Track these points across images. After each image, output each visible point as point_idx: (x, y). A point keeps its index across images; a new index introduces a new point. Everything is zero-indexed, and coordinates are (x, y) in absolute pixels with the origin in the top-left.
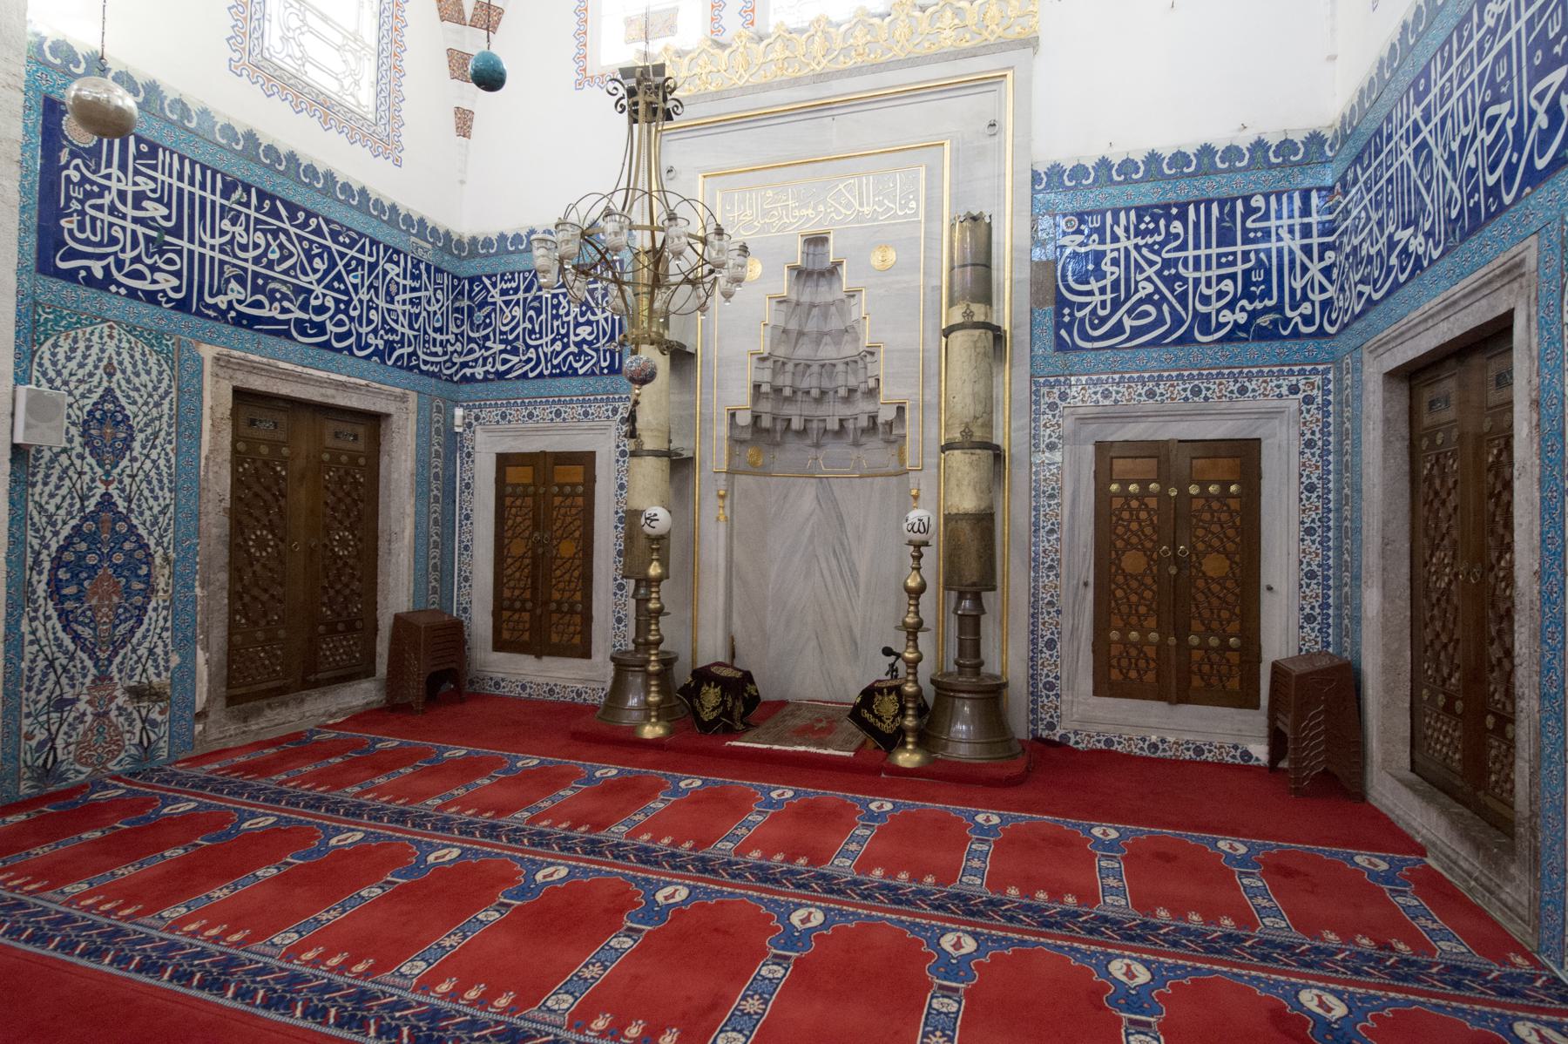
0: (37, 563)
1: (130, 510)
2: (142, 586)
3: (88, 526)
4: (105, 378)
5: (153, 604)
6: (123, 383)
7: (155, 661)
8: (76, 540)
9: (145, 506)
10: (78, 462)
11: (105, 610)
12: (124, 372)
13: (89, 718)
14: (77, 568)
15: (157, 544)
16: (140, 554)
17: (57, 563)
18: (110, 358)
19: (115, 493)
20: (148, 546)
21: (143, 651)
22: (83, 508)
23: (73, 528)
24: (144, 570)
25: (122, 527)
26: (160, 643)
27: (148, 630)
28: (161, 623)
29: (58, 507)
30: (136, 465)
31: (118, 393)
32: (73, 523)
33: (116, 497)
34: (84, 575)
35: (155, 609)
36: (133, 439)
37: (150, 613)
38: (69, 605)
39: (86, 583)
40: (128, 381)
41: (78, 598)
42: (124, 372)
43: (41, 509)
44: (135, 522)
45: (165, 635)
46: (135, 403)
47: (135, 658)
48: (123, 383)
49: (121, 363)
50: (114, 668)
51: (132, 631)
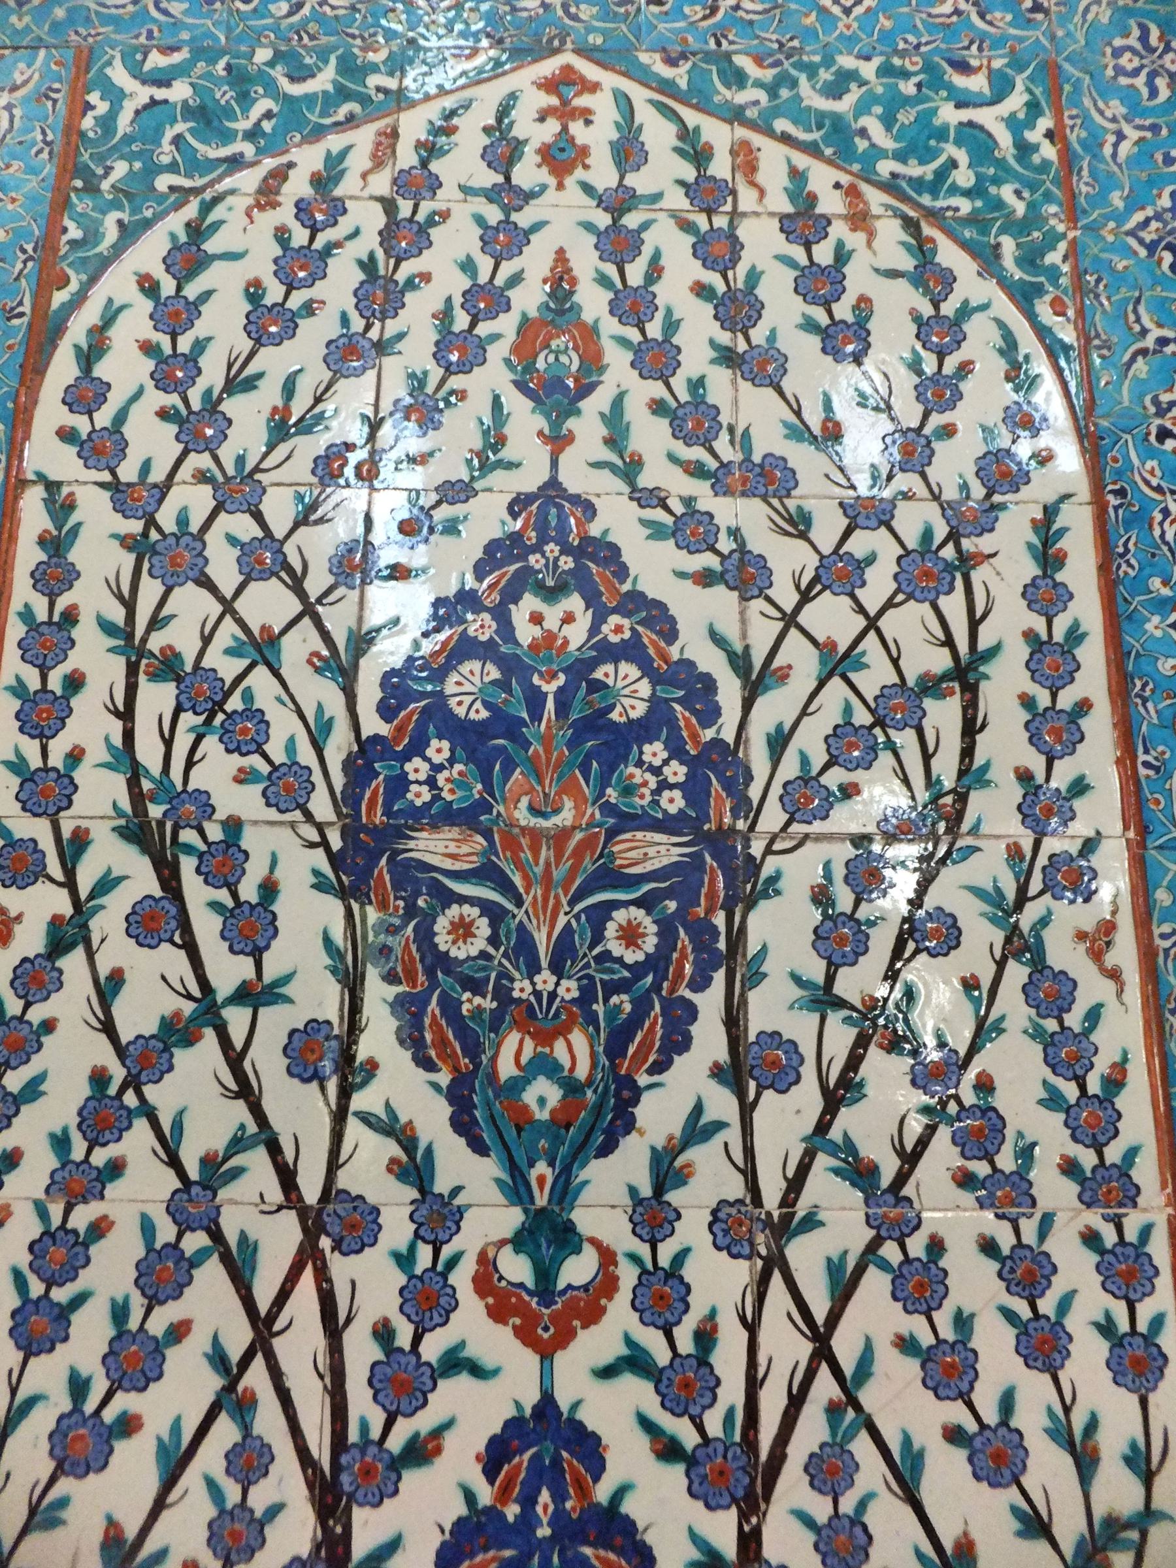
4: (525, 422)
6: (651, 437)
10: (299, 1111)
12: (657, 359)
18: (561, 281)
30: (785, 1119)
31: (618, 519)
33: (628, 1461)
36: (749, 886)
40: (693, 419)
42: (657, 359)
46: (745, 575)
48: (651, 437)
49: (633, 305)
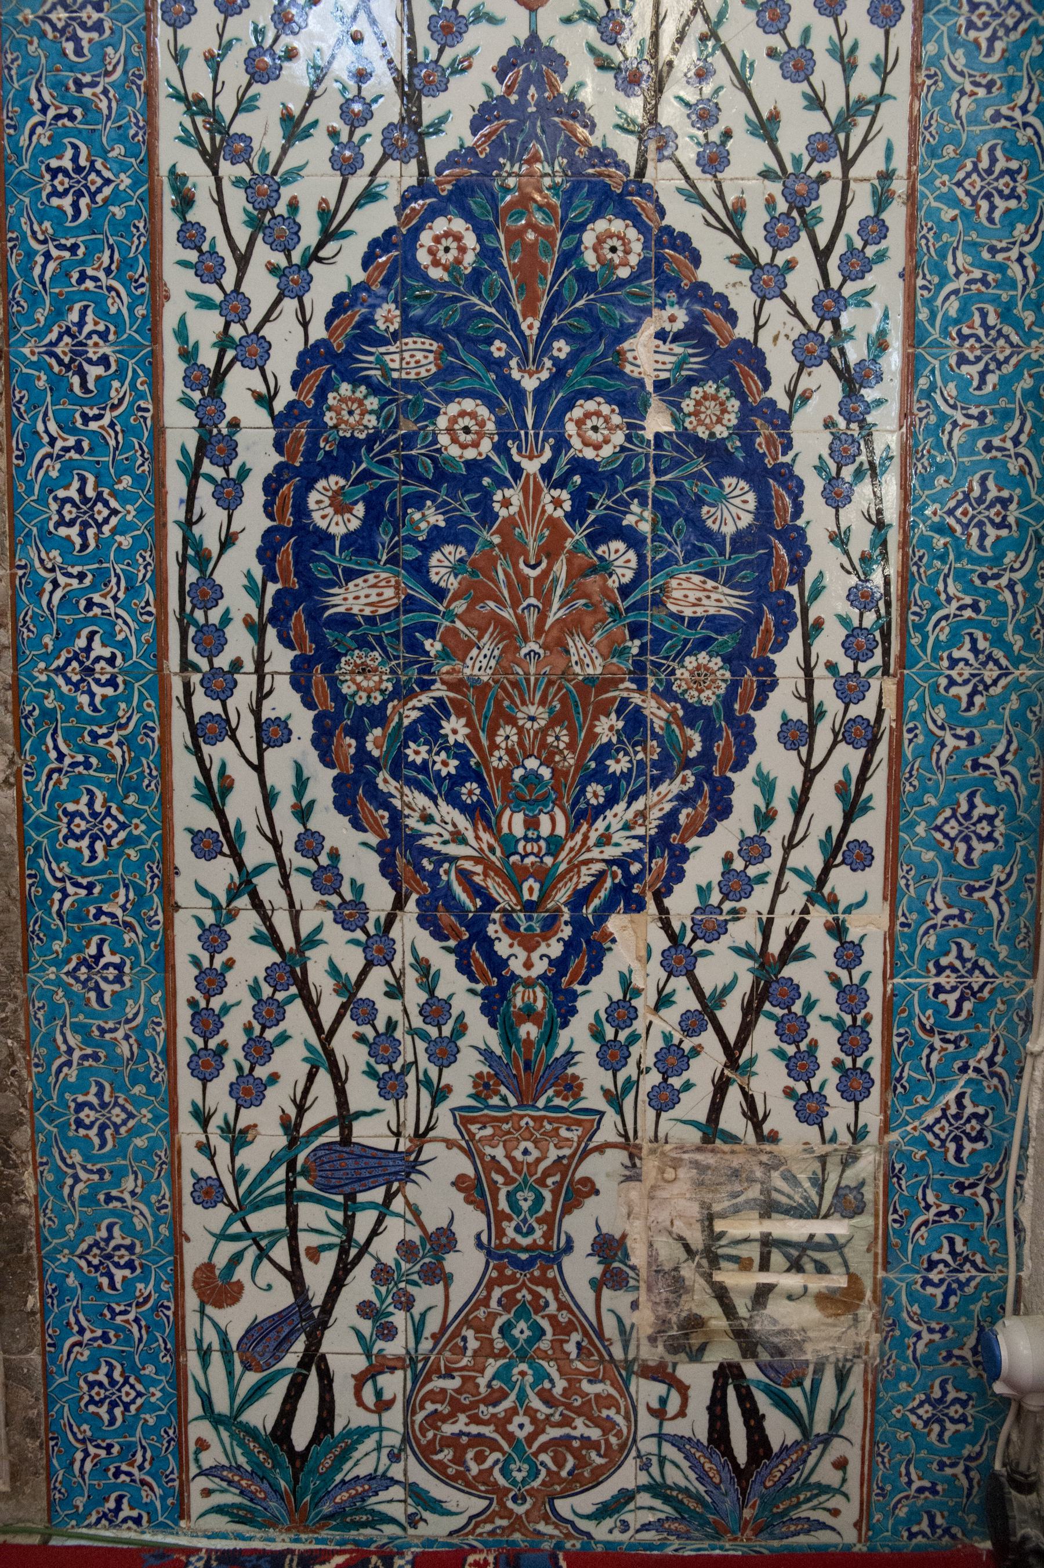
0: (215, 442)
1: (651, 132)
2: (722, 600)
3: (448, 244)
5: (784, 702)
7: (792, 1029)
8: (387, 316)
9: (734, 110)
11: (534, 714)
13: (466, 1266)
14: (395, 476)
15: (808, 353)
16: (715, 414)
17: (309, 453)
19: (573, 43)
20: (755, 358)
21: (722, 966)
22: (410, 135)
23: (377, 247)
24: (734, 510)
25: (611, 243)
26: (816, 936)
27: (754, 848)
28: (825, 809)
29: (295, 128)
32: (376, 220)
34: (433, 517)
35: (796, 736)
37: (771, 755)
38: (364, 679)
39: (441, 564)
41: (404, 636)
43: (219, 143)
44: (682, 216)
45: (844, 883)
47: (686, 1001)
50: (576, 1034)
51: (669, 845)
